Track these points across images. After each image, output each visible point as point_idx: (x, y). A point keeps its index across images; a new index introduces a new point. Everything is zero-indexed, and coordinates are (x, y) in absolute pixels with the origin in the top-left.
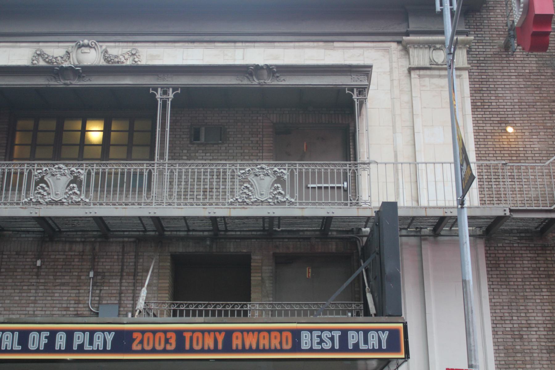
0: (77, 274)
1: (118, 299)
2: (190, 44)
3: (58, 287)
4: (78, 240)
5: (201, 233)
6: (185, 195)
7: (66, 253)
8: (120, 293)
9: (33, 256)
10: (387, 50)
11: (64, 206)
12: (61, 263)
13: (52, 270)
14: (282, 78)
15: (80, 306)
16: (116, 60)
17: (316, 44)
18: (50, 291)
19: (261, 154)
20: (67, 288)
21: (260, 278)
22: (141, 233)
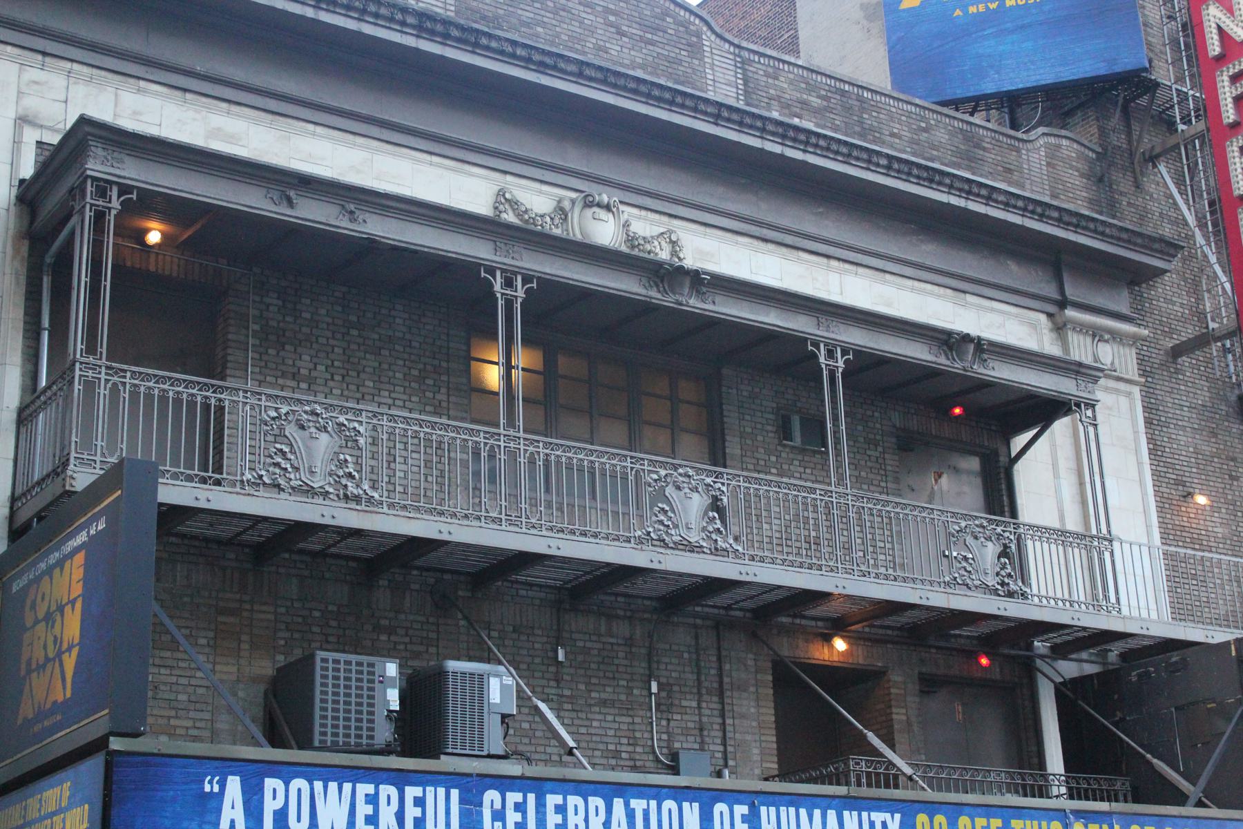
0: (624, 683)
1: (698, 740)
2: (761, 245)
3: (597, 709)
4: (621, 613)
5: (813, 623)
6: (782, 548)
7: (604, 639)
8: (701, 730)
9: (545, 639)
10: (1034, 326)
11: (702, 555)
12: (595, 659)
13: (582, 672)
14: (996, 364)
15: (639, 749)
16: (648, 247)
17: (942, 290)
18: (583, 715)
19: (883, 484)
20: (612, 711)
21: (904, 718)
22: (722, 612)
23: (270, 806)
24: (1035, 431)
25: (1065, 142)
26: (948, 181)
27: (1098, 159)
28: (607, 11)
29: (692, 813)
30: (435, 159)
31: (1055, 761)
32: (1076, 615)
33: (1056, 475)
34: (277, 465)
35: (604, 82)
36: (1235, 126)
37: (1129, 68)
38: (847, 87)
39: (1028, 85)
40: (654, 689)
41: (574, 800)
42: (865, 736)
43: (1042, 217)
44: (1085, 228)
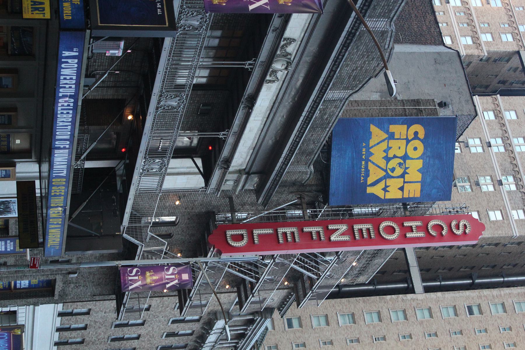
23: (69, 61)
24: (202, 169)
25: (308, 176)
26: (286, 163)
27: (301, 184)
28: (362, 67)
29: (68, 137)
30: (307, 25)
31: (89, 165)
32: (138, 169)
33: (188, 168)
34: (188, 13)
35: (329, 76)
36: (302, 230)
37: (330, 200)
38: (330, 125)
39: (331, 166)
40: (116, 72)
41: (71, 116)
42: (95, 141)
43: (277, 175)
44: (272, 185)
